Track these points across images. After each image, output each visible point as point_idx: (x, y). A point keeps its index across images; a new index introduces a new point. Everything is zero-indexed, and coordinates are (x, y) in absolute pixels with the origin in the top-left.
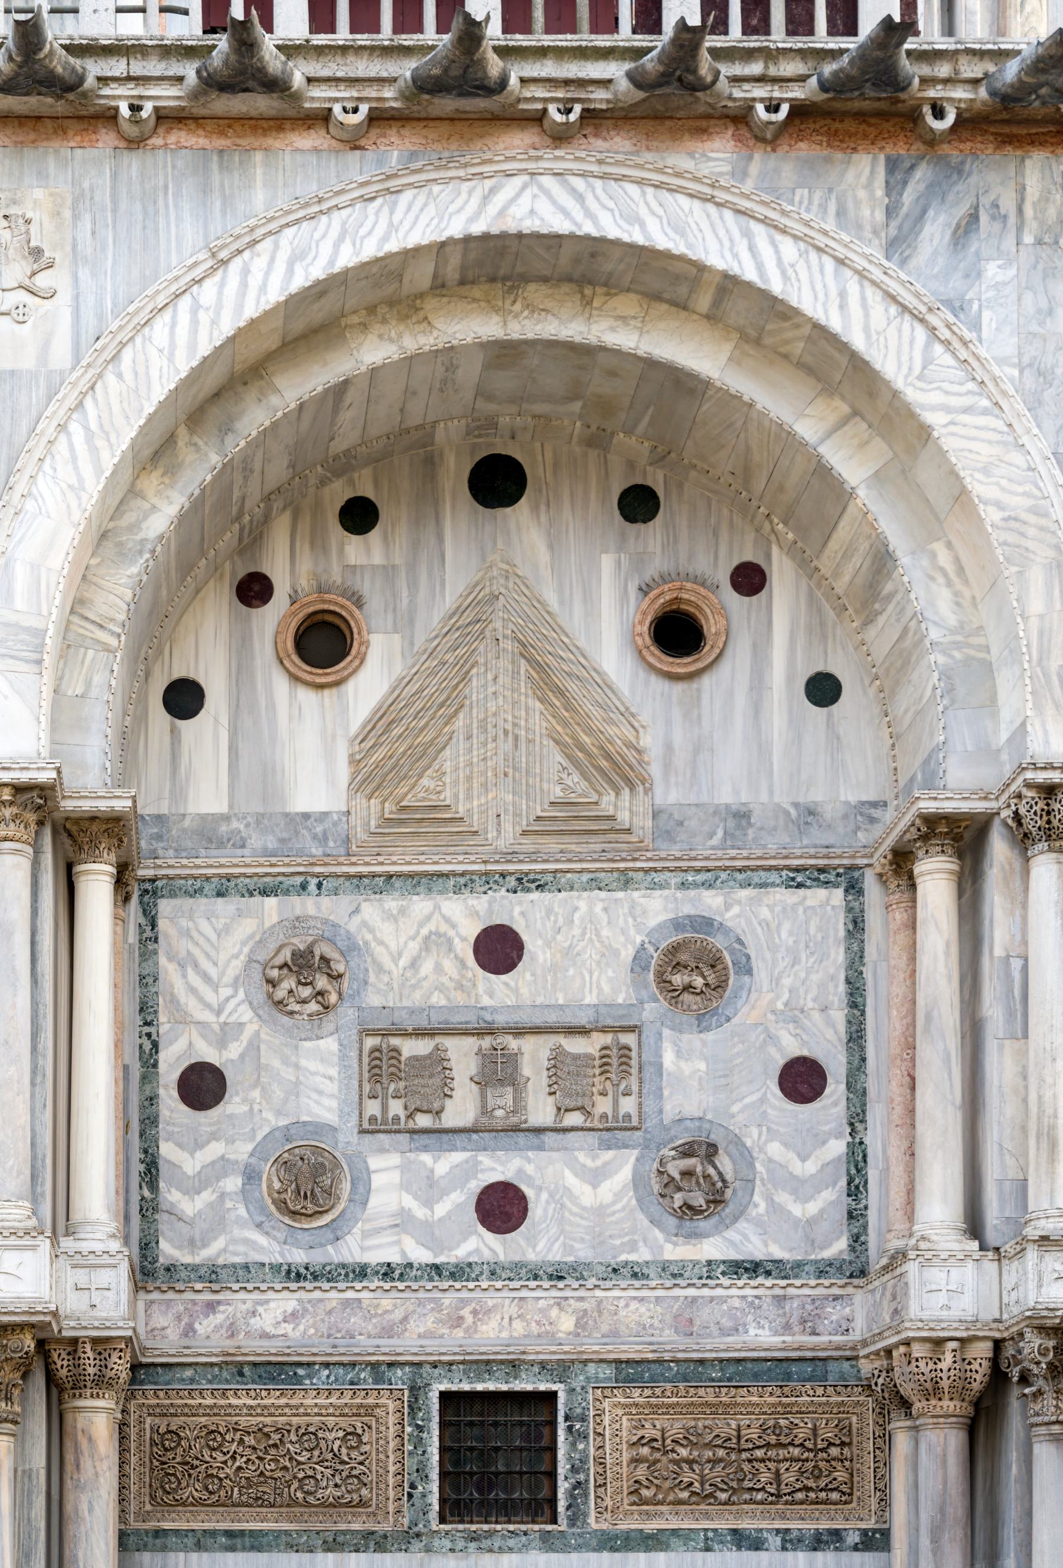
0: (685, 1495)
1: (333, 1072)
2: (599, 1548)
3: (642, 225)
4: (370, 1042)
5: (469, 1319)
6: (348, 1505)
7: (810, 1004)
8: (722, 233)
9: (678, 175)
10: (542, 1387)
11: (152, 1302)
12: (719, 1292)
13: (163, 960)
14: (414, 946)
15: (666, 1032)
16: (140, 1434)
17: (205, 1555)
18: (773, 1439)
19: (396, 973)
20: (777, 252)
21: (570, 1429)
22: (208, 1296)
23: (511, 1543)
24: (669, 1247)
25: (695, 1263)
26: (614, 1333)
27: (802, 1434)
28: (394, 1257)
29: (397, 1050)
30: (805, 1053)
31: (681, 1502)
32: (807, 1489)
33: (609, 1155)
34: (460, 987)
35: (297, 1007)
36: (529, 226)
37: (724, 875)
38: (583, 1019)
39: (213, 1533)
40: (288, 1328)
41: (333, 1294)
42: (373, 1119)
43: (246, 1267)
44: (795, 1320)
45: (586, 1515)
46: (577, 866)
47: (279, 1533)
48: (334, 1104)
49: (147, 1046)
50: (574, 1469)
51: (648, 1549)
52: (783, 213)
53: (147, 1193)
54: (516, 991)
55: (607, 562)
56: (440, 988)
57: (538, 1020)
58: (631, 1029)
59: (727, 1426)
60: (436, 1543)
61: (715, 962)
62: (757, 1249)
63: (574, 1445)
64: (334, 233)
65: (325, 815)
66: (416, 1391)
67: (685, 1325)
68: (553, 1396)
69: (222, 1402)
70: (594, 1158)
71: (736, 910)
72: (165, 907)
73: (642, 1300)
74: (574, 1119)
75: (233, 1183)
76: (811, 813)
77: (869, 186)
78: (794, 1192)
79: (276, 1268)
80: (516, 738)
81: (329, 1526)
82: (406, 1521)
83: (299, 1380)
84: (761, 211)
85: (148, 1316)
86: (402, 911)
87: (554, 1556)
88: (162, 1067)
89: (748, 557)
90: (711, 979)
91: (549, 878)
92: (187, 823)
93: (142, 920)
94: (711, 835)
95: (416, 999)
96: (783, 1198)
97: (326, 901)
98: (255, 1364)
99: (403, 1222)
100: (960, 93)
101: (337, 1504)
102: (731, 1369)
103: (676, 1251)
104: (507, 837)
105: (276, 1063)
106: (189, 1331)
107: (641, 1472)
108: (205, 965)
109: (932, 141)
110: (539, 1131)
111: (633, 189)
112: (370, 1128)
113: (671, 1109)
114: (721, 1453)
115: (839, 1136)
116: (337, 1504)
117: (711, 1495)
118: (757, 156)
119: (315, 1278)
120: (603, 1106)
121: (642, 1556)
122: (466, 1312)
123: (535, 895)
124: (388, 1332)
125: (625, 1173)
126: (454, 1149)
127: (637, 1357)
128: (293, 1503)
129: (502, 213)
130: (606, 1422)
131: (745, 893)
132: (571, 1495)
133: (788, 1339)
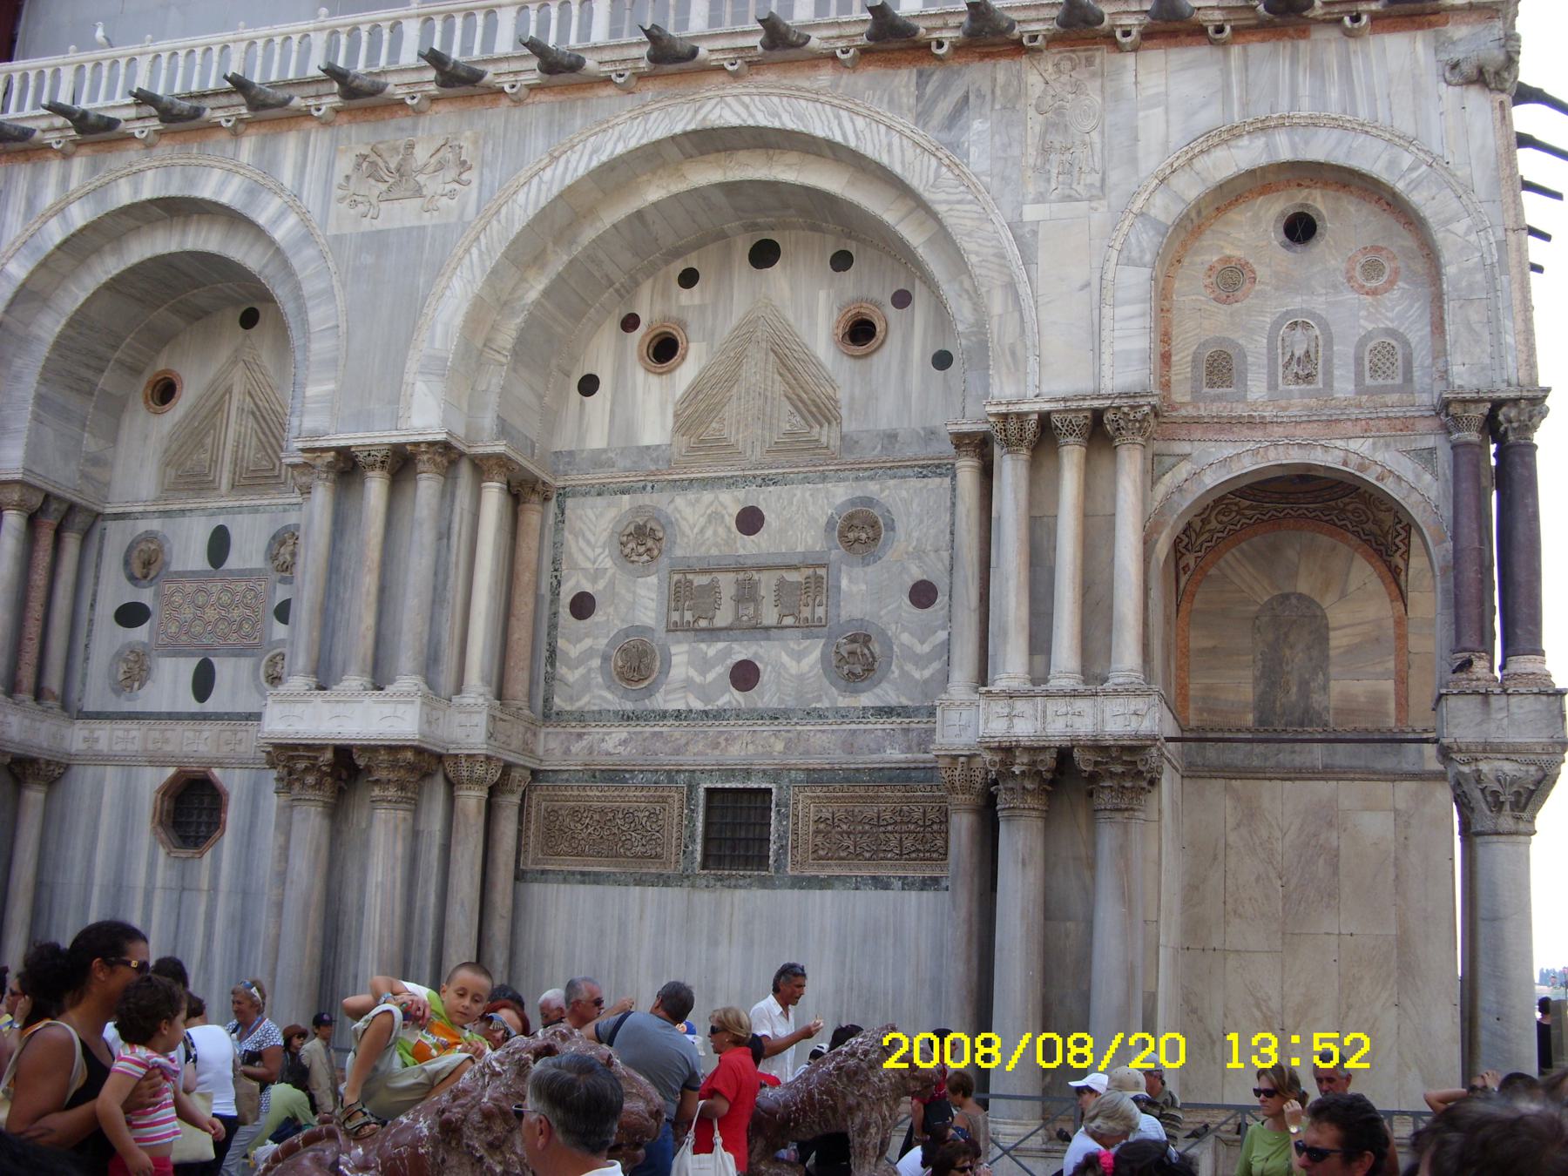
0: (843, 854)
1: (654, 596)
2: (793, 887)
4: (676, 577)
5: (723, 744)
7: (929, 548)
8: (824, 118)
9: (798, 90)
10: (763, 786)
11: (548, 733)
12: (870, 726)
13: (566, 533)
14: (702, 521)
15: (844, 567)
17: (568, 886)
18: (899, 819)
19: (692, 536)
20: (854, 124)
22: (578, 730)
23: (741, 882)
24: (840, 698)
25: (855, 709)
26: (807, 752)
28: (681, 706)
29: (691, 582)
30: (925, 577)
32: (918, 850)
35: (636, 558)
37: (880, 472)
38: (795, 562)
39: (573, 873)
40: (621, 749)
41: (647, 729)
43: (600, 712)
45: (786, 866)
46: (796, 470)
47: (609, 875)
48: (653, 615)
49: (555, 583)
51: (821, 888)
52: (857, 105)
53: (549, 669)
54: (758, 545)
55: (822, 295)
56: (716, 545)
57: (770, 563)
59: (871, 811)
60: (698, 882)
61: (874, 525)
63: (780, 822)
64: (614, 138)
66: (692, 788)
67: (849, 748)
68: (769, 791)
69: (583, 794)
70: (799, 644)
71: (887, 492)
72: (570, 503)
73: (823, 731)
74: (789, 621)
75: (596, 663)
77: (907, 86)
78: (916, 664)
79: (616, 713)
80: (766, 398)
81: (637, 870)
82: (681, 868)
83: (625, 780)
85: (546, 741)
86: (698, 500)
87: (766, 891)
88: (562, 595)
89: (902, 287)
90: (870, 535)
91: (780, 477)
92: (585, 455)
93: (557, 511)
94: (874, 449)
95: (702, 551)
96: (909, 667)
98: (603, 771)
99: (688, 685)
102: (876, 775)
103: (843, 702)
104: (757, 455)
105: (623, 591)
106: (567, 751)
107: (819, 839)
108: (588, 534)
109: (939, 58)
110: (767, 628)
112: (673, 628)
113: (844, 615)
114: (867, 827)
117: (860, 854)
118: (845, 76)
119: (638, 719)
120: (806, 612)
122: (721, 740)
123: (771, 488)
124: (677, 751)
125: (816, 654)
126: (719, 640)
127: (819, 767)
129: (704, 119)
131: (892, 482)
132: (777, 854)
133: (909, 756)
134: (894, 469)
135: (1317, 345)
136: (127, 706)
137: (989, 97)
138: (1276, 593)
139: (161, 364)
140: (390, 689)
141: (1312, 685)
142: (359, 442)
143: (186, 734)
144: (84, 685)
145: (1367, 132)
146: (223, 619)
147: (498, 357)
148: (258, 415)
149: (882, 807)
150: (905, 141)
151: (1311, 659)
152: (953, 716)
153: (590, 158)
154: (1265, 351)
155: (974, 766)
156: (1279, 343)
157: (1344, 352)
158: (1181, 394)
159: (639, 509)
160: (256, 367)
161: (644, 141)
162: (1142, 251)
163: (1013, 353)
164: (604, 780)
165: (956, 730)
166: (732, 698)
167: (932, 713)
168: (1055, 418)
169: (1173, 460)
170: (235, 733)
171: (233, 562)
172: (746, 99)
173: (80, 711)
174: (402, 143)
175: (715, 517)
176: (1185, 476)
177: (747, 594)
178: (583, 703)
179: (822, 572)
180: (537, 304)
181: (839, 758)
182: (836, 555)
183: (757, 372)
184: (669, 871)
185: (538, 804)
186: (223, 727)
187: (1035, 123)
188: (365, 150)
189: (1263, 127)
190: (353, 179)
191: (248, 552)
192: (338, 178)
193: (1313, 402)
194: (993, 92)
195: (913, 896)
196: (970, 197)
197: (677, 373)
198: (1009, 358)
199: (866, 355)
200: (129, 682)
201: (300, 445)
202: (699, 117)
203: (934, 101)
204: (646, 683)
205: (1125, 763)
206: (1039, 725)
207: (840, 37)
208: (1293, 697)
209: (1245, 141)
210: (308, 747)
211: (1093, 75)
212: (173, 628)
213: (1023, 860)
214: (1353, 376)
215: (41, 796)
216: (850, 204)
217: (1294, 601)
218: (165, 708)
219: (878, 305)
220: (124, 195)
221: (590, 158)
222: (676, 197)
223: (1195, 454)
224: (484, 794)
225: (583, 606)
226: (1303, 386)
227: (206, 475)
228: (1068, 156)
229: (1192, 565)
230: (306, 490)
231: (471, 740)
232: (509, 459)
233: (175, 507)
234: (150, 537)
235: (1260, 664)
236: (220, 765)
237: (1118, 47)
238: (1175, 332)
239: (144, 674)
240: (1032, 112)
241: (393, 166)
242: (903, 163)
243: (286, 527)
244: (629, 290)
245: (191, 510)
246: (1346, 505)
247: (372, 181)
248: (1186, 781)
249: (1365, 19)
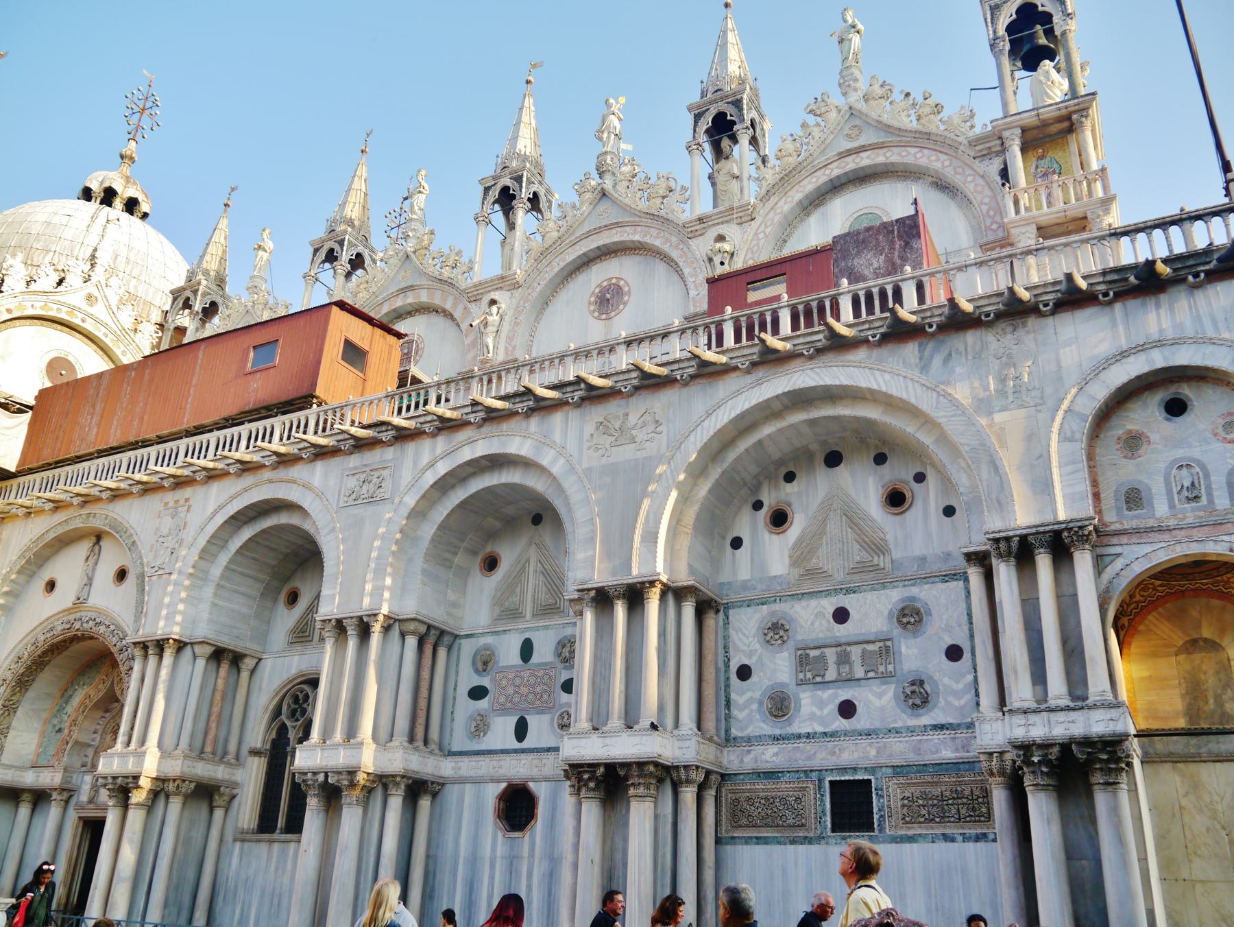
0: (923, 820)
1: (787, 664)
2: (891, 842)
3: (839, 378)
4: (799, 652)
5: (838, 752)
6: (798, 826)
13: (731, 630)
14: (812, 617)
15: (902, 640)
16: (726, 800)
18: (955, 796)
21: (877, 794)
26: (891, 755)
27: (967, 793)
28: (809, 730)
31: (920, 823)
33: (884, 687)
34: (828, 630)
36: (802, 386)
38: (872, 638)
39: (751, 838)
40: (774, 759)
42: (801, 680)
44: (960, 747)
48: (787, 675)
50: (880, 810)
55: (871, 480)
57: (856, 639)
58: (889, 640)
59: (936, 791)
61: (918, 613)
62: (942, 720)
65: (781, 576)
66: (820, 781)
67: (917, 750)
68: (870, 781)
72: (731, 612)
75: (755, 706)
76: (949, 555)
79: (770, 736)
84: (876, 367)
86: (808, 606)
95: (814, 636)
97: (783, 605)
99: (812, 717)
100: (936, 319)
101: (794, 826)
102: (937, 767)
103: (912, 722)
104: (840, 576)
106: (742, 761)
108: (744, 630)
110: (859, 680)
111: (835, 369)
112: (801, 683)
114: (935, 802)
115: (970, 673)
116: (794, 826)
120: (882, 669)
121: (908, 845)
122: (837, 750)
123: (853, 595)
124: (809, 758)
125: (891, 694)
128: (778, 826)
130: (891, 790)
131: (927, 586)
132: (879, 821)
134: (927, 579)
135: (1199, 478)
136: (476, 747)
137: (964, 353)
138: (1187, 639)
139: (489, 549)
140: (636, 727)
141: (1224, 697)
142: (610, 584)
145: (1214, 343)
146: (530, 692)
147: (686, 530)
148: (545, 573)
149: (944, 788)
150: (916, 384)
151: (1220, 680)
152: (986, 727)
153: (730, 413)
154: (1163, 485)
155: (1004, 759)
156: (1173, 480)
157: (1219, 481)
158: (1110, 517)
159: (773, 613)
161: (761, 400)
162: (1073, 432)
163: (999, 502)
164: (766, 778)
165: (989, 736)
166: (841, 724)
167: (970, 726)
168: (1030, 538)
169: (1112, 557)
170: (541, 760)
171: (535, 659)
172: (818, 370)
173: (449, 751)
174: (621, 413)
175: (819, 615)
176: (1120, 567)
177: (844, 659)
178: (750, 731)
179: (888, 643)
180: (706, 498)
181: (912, 758)
182: (897, 631)
183: (835, 526)
184: (811, 834)
185: (726, 795)
187: (995, 365)
188: (601, 419)
189: (1141, 348)
190: (595, 436)
191: (544, 652)
192: (587, 436)
193: (1202, 513)
194: (966, 349)
195: (971, 845)
196: (960, 412)
197: (788, 531)
198: (996, 505)
199: (902, 513)
200: (477, 733)
201: (576, 588)
202: (791, 383)
203: (931, 357)
204: (786, 717)
205: (1108, 753)
206: (1047, 730)
207: (869, 329)
208: (1212, 707)
209: (1132, 359)
210: (590, 765)
211: (1028, 332)
212: (502, 700)
213: (1048, 819)
214: (1227, 494)
215: (429, 803)
216: (885, 424)
217: (1201, 643)
219: (903, 482)
220: (467, 455)
221: (730, 413)
222: (780, 430)
223: (1125, 553)
224: (695, 789)
225: (744, 673)
226: (1194, 504)
228: (1018, 381)
229: (1126, 624)
230: (580, 614)
231: (685, 756)
232: (696, 589)
234: (487, 647)
235: (1184, 685)
236: (534, 780)
237: (1040, 314)
238: (1100, 479)
240: (992, 359)
241: (617, 426)
242: (916, 397)
244: (757, 488)
246: (1229, 578)
247: (606, 436)
248: (1145, 765)
249: (1202, 275)
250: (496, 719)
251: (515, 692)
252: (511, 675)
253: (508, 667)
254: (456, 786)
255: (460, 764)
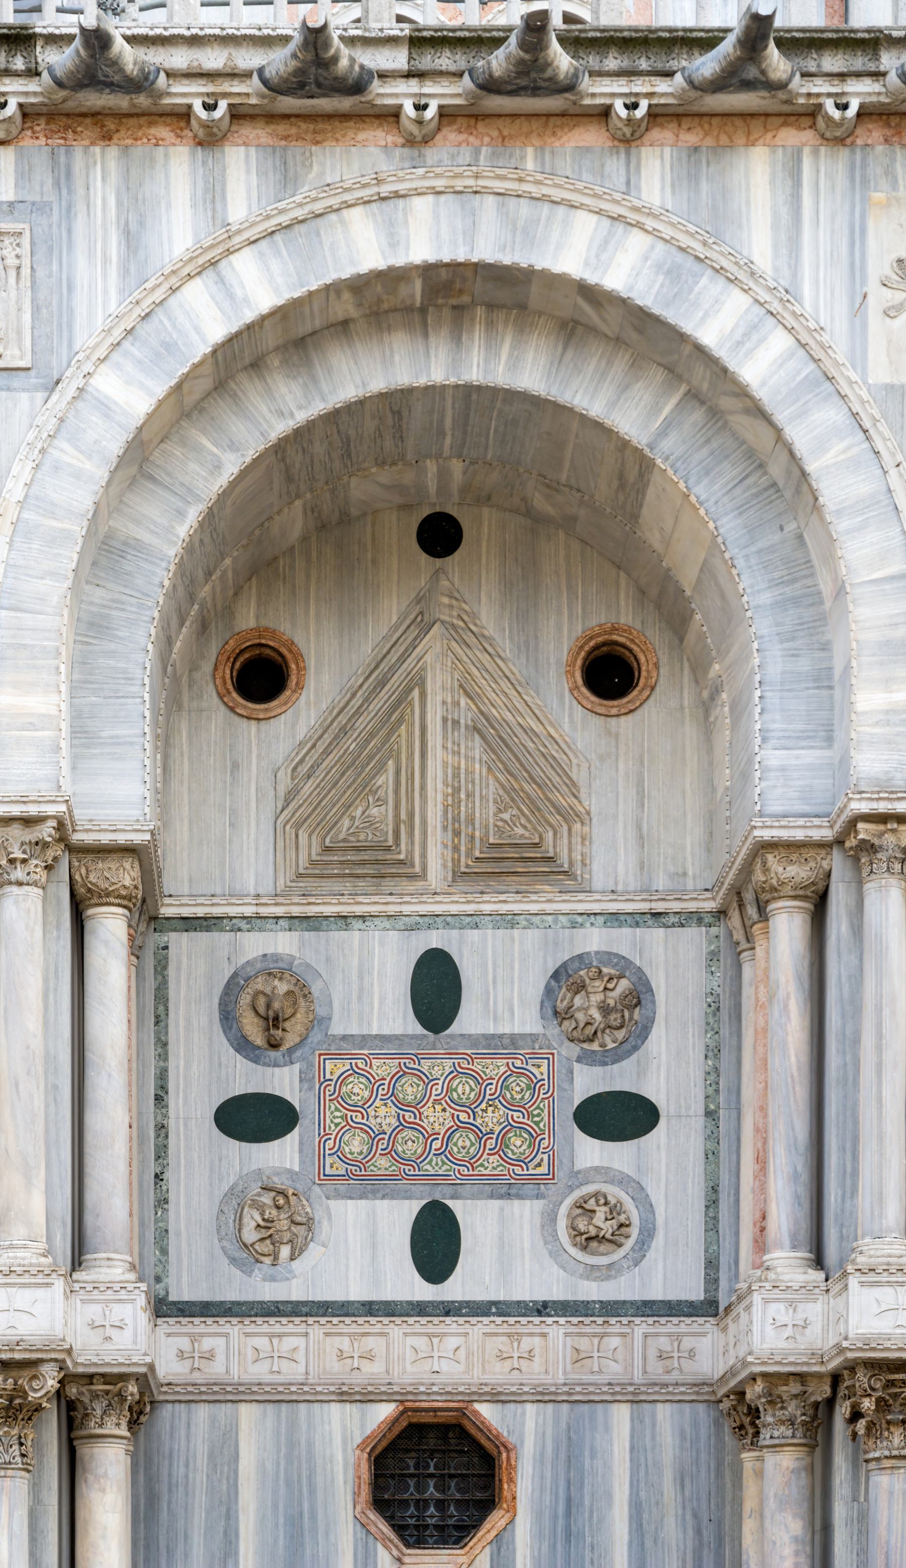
136: (269, 1292)
143: (410, 1341)
144: (164, 1251)
160: (471, 640)
186: (492, 1329)
200: (266, 1247)
212: (356, 1145)
218: (356, 1293)
227: (388, 849)
233: (327, 910)
236: (496, 1398)
239: (301, 1231)
243: (580, 957)
245: (363, 918)
250: (335, 1205)
251: (402, 1125)
252: (382, 1069)
253: (365, 1040)
254: (202, 1412)
255: (207, 1344)
